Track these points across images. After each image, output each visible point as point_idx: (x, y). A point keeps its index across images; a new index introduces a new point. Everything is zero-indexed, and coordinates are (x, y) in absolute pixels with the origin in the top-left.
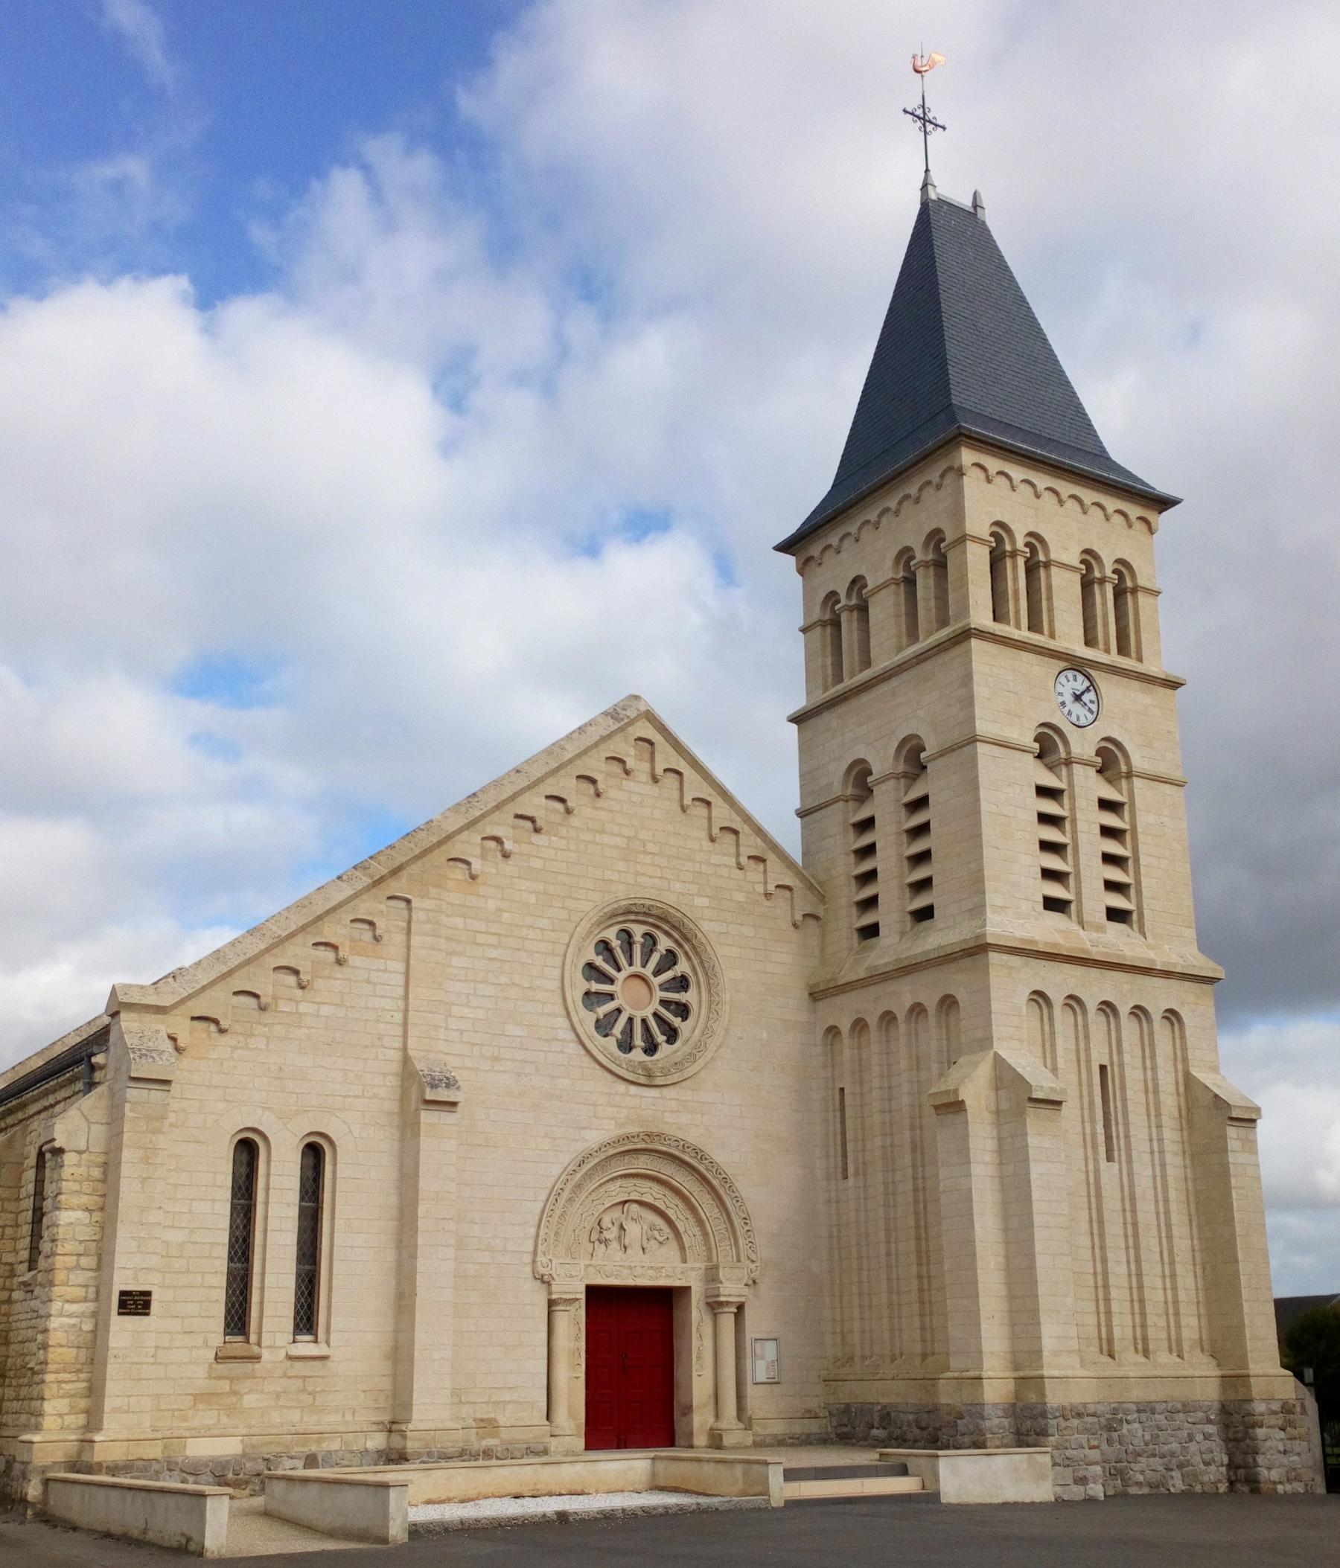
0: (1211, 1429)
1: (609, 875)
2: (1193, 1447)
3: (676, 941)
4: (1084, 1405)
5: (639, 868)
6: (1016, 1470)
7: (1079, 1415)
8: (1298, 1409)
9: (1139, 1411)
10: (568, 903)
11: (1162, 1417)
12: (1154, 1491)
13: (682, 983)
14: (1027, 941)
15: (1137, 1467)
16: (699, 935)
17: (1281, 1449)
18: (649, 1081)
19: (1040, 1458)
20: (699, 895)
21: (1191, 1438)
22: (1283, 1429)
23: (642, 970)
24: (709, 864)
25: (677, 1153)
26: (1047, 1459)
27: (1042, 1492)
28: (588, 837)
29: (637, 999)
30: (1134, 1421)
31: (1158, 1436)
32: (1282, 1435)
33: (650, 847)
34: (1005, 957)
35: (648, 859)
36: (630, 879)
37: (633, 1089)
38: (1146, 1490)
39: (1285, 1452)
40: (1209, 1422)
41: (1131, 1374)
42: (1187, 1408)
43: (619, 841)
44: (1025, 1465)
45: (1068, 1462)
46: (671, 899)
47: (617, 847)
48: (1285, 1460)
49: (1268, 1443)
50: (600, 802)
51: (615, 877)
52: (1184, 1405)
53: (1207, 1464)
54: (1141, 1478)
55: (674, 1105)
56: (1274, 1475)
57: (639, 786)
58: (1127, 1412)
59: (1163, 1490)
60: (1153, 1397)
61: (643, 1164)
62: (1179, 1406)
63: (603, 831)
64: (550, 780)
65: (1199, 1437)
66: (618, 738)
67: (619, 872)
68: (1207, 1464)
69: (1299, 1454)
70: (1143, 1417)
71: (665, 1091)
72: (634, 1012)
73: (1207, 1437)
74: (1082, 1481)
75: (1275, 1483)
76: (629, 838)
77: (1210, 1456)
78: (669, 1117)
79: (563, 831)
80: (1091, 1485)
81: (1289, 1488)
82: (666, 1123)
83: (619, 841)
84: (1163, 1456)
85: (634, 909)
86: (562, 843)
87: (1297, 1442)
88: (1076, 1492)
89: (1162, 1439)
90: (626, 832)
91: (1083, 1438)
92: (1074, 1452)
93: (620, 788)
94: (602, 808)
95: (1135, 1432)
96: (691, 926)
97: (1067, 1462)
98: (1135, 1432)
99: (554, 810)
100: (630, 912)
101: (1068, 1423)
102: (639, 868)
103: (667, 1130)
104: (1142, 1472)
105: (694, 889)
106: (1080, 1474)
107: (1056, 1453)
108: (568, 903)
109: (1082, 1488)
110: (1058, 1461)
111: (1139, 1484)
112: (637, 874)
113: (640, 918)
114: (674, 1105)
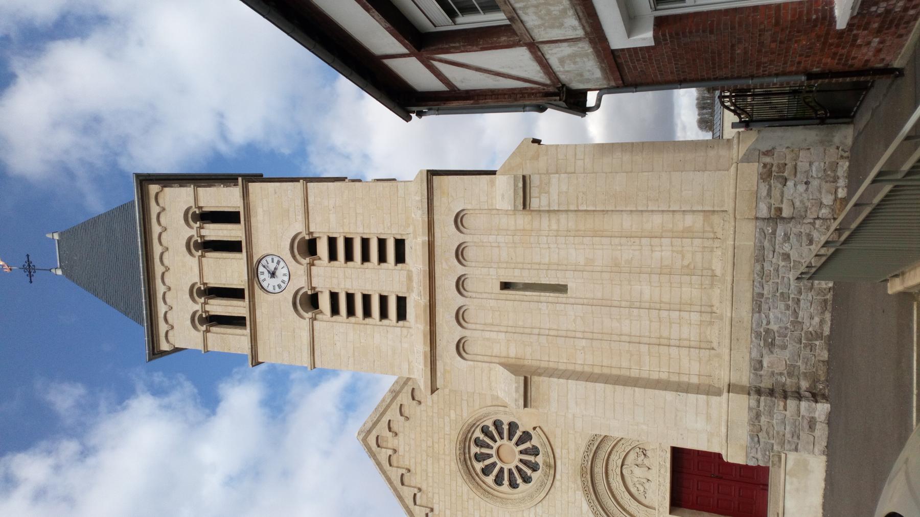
0: (780, 232)
1: (447, 472)
2: (794, 256)
4: (750, 409)
5: (441, 452)
6: (797, 490)
7: (758, 416)
8: (767, 160)
9: (759, 312)
10: (465, 497)
12: (829, 307)
13: (497, 424)
14: (425, 357)
15: (807, 322)
17: (804, 187)
18: (552, 467)
20: (449, 416)
21: (787, 257)
22: (786, 180)
24: (432, 407)
26: (792, 457)
27: (817, 465)
28: (430, 480)
29: (509, 455)
30: (767, 317)
31: (782, 294)
32: (790, 184)
34: (439, 374)
35: (436, 446)
36: (448, 458)
37: (558, 476)
38: (828, 316)
39: (807, 183)
40: (774, 233)
41: (729, 315)
42: (760, 258)
43: (430, 462)
44: (795, 480)
45: (796, 434)
47: (433, 463)
48: (815, 183)
49: (797, 204)
50: (412, 469)
51: (447, 467)
52: (757, 261)
53: (811, 242)
54: (817, 320)
56: (828, 200)
57: (400, 443)
58: (759, 325)
59: (829, 296)
60: (749, 295)
61: (599, 469)
62: (758, 267)
63: (426, 471)
64: (406, 501)
65: (787, 248)
69: (811, 164)
70: (765, 307)
71: (557, 456)
72: (517, 453)
73: (787, 238)
75: (835, 200)
76: (427, 456)
77: (804, 238)
78: (572, 456)
79: (430, 495)
80: (817, 415)
81: (842, 182)
83: (430, 462)
84: (800, 293)
85: (462, 459)
86: (436, 496)
87: (799, 164)
88: (821, 432)
89: (785, 291)
90: (424, 457)
91: (777, 417)
92: (788, 428)
93: (404, 456)
95: (777, 318)
97: (795, 438)
98: (777, 318)
99: (421, 497)
100: (465, 459)
101: (764, 428)
102: (441, 452)
103: (579, 460)
104: (812, 318)
105: (447, 419)
106: (806, 427)
107: (787, 446)
108: (465, 497)
109: (818, 426)
110: (793, 447)
111: (822, 322)
112: (444, 454)
114: (564, 451)
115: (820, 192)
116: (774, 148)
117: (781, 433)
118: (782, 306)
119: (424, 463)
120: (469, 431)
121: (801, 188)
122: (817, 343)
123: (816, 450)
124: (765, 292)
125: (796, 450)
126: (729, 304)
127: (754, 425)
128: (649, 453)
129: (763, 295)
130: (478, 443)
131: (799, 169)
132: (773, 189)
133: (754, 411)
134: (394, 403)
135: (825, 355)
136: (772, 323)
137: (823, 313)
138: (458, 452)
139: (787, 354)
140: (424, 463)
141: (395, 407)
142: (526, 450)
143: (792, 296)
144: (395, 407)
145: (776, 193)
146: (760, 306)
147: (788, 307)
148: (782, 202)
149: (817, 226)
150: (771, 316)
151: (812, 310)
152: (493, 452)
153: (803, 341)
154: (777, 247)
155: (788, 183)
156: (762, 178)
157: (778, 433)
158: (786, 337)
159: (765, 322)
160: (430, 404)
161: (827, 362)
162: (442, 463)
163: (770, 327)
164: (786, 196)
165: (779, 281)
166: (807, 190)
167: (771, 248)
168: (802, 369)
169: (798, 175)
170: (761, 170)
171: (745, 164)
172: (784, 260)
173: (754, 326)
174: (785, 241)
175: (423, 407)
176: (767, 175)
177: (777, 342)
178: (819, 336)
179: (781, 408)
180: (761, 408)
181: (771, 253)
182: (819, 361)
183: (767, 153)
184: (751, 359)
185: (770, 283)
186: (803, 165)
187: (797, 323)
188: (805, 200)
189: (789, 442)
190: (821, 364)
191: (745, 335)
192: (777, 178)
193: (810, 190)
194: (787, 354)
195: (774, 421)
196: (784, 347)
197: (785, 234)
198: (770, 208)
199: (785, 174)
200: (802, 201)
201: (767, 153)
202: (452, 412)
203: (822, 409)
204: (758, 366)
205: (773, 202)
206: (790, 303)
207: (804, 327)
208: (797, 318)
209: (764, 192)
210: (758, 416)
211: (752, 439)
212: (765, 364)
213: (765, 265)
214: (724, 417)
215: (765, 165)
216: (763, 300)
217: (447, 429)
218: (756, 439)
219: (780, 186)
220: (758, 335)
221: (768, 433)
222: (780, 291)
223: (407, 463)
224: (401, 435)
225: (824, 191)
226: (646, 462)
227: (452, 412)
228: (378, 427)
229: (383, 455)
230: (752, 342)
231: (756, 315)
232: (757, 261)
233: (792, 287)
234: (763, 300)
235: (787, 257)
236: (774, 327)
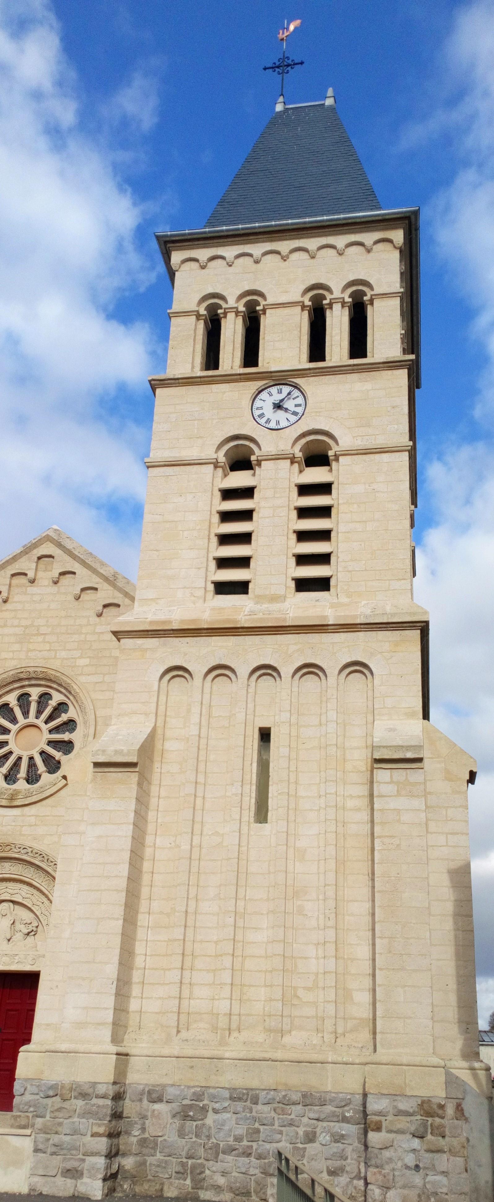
2: (312, 1149)
3: (66, 696)
4: (94, 1084)
5: (31, 647)
7: (84, 1096)
8: (450, 1111)
9: (232, 1098)
11: (266, 1108)
13: (70, 725)
16: (75, 687)
17: (412, 1164)
19: (15, 1141)
21: (311, 1138)
23: (27, 721)
25: (28, 859)
26: (27, 1144)
31: (258, 1131)
32: (416, 1143)
33: (43, 630)
35: (40, 639)
40: (345, 1120)
41: (227, 1055)
42: (308, 1099)
43: (18, 630)
46: (55, 664)
48: (417, 1179)
49: (387, 1154)
50: (8, 606)
51: (11, 655)
52: (304, 1096)
54: (221, 1181)
55: (33, 820)
58: (213, 1098)
60: (255, 1083)
62: (296, 1097)
63: (5, 626)
66: (23, 560)
67: (13, 652)
68: (332, 1173)
70: (239, 1106)
72: (30, 753)
73: (338, 1138)
74: (73, 1173)
76: (26, 627)
77: (338, 1163)
80: (85, 1180)
82: (24, 835)
83: (18, 630)
84: (259, 1157)
85: (22, 676)
87: (445, 1156)
88: (63, 1187)
89: (262, 1136)
90: (24, 623)
91: (83, 1124)
92: (67, 1138)
94: (6, 610)
95: (224, 1124)
96: (69, 681)
97: (54, 1149)
98: (224, 1124)
101: (66, 1105)
103: (21, 841)
104: (224, 1174)
106: (69, 1165)
107: (41, 1137)
109: (70, 1182)
110: (41, 1146)
111: (218, 1189)
113: (33, 682)
114: (33, 820)
115: (404, 1187)
116: (466, 1120)
117: (60, 1129)
118: (241, 1130)
119: (16, 622)
120: (60, 685)
121: (410, 1160)
122: (188, 1182)
123: (36, 1179)
124: (260, 1107)
125: (36, 1150)
126: (241, 1056)
127: (71, 1090)
128: (30, 939)
129: (256, 1103)
130: (44, 698)
131: (437, 1156)
132: (409, 1119)
133: (90, 1091)
134: (98, 580)
135: (171, 1192)
136: (216, 1116)
137: (231, 1189)
138: (31, 670)
139: (172, 1137)
140: (16, 622)
141: (94, 581)
142: (35, 765)
143: (254, 1145)
144: (94, 581)
145: (403, 1123)
146: (240, 1099)
147: (238, 1139)
148: (390, 1131)
149: (355, 1182)
150: (226, 1116)
151: (235, 1174)
152: (32, 719)
153: (190, 1162)
154: (325, 1124)
155: (417, 1141)
156: (423, 1102)
157: (60, 1124)
158: (197, 1136)
159: (217, 1106)
160: (99, 629)
161: (161, 1196)
162: (16, 647)
163: (210, 1114)
164: (399, 1137)
165: (276, 1127)
166: (407, 1167)
167: (322, 1116)
168: (150, 1160)
169: (428, 1155)
170: (435, 1101)
171: (443, 1079)
172: (306, 1134)
173: (211, 1091)
174: (332, 1135)
175: (94, 619)
176: (428, 1109)
177: (188, 1123)
178: (198, 1184)
179: (96, 1129)
180: (95, 1101)
181: (316, 1116)
182: (162, 1184)
183: (459, 1109)
184: (164, 1086)
185: (273, 1114)
186: (443, 1161)
187: (216, 1152)
188: (392, 1166)
189: (48, 1140)
190: (158, 1187)
191: (198, 1078)
192: (424, 1125)
193: (408, 1172)
194: (172, 1137)
195: (76, 1119)
196: (181, 1134)
197: (343, 1136)
198: (380, 1113)
199: (429, 1137)
200: (390, 1160)
201: (459, 1109)
202: (86, 661)
203: (95, 1188)
204: (154, 1096)
205: (390, 1118)
206: (245, 1143)
207: (211, 1163)
208: (224, 1153)
209: (403, 1106)
210: (84, 1096)
211: (51, 1087)
212: (157, 1106)
213: (299, 1107)
214: (81, 1048)
215: (442, 1107)
216: (248, 1103)
217: (63, 654)
218: (51, 1093)
219: (413, 1129)
220: (198, 1097)
221: (59, 1110)
222: (262, 1128)
223: (17, 598)
224: (55, 589)
225: (406, 1192)
226: (18, 936)
227: (86, 661)
228: (67, 558)
229: (27, 565)
230: (189, 1087)
231: (227, 1094)
232: (304, 1096)
233: (268, 1146)
234: (248, 1103)
235: (311, 1138)
236: (210, 1119)
